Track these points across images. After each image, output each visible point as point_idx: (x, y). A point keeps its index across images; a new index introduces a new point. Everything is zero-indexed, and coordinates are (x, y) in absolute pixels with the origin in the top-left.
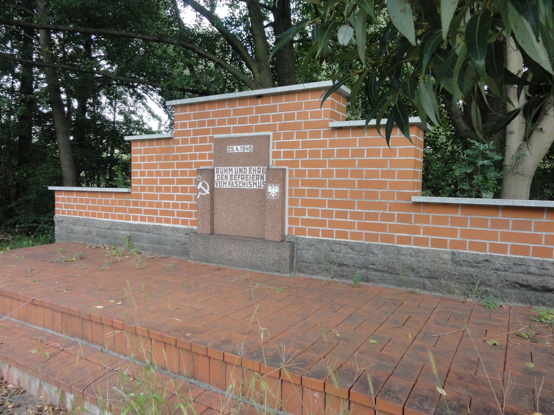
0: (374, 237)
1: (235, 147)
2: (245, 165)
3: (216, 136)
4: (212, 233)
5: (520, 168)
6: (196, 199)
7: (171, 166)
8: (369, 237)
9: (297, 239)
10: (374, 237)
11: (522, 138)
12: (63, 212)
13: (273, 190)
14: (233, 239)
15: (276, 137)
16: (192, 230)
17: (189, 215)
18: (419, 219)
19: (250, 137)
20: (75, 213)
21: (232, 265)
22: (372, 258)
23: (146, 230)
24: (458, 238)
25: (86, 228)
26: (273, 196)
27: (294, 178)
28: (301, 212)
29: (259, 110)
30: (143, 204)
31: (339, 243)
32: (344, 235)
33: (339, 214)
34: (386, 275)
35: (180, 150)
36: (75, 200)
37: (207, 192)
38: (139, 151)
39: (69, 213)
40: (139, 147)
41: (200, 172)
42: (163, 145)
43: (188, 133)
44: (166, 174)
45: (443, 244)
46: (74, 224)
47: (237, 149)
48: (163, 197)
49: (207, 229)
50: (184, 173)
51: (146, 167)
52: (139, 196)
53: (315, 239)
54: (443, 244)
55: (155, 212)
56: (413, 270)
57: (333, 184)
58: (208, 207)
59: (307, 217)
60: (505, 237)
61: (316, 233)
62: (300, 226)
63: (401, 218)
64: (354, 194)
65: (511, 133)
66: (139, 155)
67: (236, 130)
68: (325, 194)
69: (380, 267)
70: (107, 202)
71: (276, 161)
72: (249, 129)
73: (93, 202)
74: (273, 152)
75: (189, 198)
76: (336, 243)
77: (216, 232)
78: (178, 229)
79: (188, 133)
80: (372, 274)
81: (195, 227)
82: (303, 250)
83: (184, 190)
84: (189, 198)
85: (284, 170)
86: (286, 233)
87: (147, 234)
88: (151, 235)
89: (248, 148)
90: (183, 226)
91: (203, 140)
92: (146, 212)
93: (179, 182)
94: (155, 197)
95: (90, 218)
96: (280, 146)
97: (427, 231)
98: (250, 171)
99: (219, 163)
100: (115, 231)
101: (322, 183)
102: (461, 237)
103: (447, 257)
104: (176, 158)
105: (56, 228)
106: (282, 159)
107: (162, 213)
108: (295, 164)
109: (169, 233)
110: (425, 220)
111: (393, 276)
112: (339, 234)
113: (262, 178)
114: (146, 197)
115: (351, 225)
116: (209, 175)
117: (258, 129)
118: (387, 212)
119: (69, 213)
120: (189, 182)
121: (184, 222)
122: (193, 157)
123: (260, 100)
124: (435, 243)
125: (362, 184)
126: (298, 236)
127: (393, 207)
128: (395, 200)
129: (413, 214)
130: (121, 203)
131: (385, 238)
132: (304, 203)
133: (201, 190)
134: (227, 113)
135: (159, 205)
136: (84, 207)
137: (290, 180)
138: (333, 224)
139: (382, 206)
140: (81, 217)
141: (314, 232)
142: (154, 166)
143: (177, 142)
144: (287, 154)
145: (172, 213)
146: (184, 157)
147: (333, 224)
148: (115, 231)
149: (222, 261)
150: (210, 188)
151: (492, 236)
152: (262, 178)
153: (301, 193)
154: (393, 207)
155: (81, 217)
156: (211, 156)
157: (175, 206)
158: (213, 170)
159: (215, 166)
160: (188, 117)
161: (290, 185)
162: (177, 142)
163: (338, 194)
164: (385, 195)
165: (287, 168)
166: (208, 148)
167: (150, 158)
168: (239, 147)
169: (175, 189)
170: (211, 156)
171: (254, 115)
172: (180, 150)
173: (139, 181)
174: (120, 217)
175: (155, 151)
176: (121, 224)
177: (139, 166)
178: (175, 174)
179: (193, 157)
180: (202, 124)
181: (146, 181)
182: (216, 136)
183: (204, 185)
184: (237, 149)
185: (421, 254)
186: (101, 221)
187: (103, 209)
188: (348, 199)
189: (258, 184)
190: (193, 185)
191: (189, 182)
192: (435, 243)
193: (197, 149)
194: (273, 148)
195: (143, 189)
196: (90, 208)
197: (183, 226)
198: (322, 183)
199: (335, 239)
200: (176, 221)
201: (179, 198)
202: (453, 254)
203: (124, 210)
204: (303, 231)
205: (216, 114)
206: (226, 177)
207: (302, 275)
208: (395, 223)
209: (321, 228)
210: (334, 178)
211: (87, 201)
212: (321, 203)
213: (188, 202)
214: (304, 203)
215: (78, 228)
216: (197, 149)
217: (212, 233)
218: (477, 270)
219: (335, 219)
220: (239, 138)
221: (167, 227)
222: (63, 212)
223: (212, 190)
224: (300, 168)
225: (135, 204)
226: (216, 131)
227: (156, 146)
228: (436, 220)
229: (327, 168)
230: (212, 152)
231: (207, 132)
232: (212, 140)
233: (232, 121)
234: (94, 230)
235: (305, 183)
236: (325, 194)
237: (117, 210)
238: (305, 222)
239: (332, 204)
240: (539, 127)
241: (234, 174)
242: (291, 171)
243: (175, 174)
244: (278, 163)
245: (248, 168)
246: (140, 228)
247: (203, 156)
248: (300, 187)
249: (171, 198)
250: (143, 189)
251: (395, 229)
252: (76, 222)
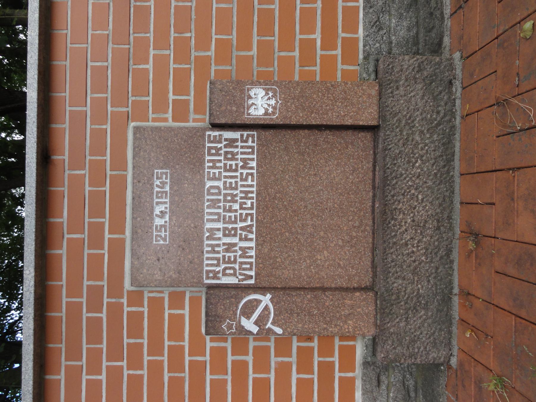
1: (158, 222)
16: (366, 364)
21: (449, 218)
26: (273, 102)
37: (266, 300)
53: (366, 14)
59: (317, 36)
62: (339, 52)
71: (196, 112)
74: (174, 120)
77: (367, 281)
82: (391, 43)
98: (214, 179)
113: (231, 143)
126: (361, 56)
149: (442, 252)
150: (255, 292)
158: (210, 287)
168: (157, 210)
171: (85, 172)
194: (166, 120)
206: (230, 247)
213: (294, 376)
223: (262, 289)
224: (212, 53)
241: (220, 225)
245: (209, 184)
248: (254, 52)
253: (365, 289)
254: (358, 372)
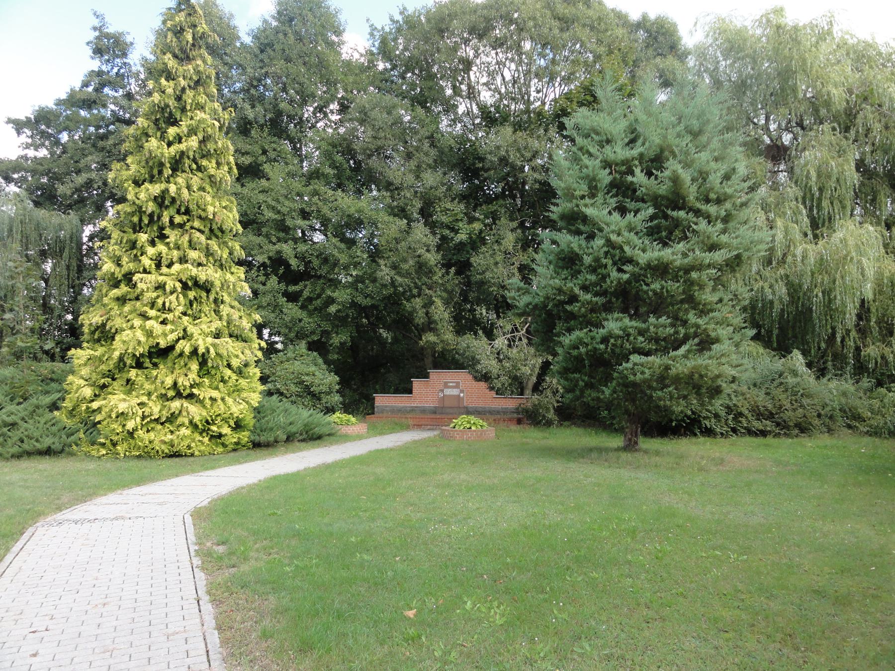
13: (462, 395)
47: (451, 384)
89: (454, 384)
116: (442, 391)
184: (451, 384)
189: (457, 393)
246: (416, 407)
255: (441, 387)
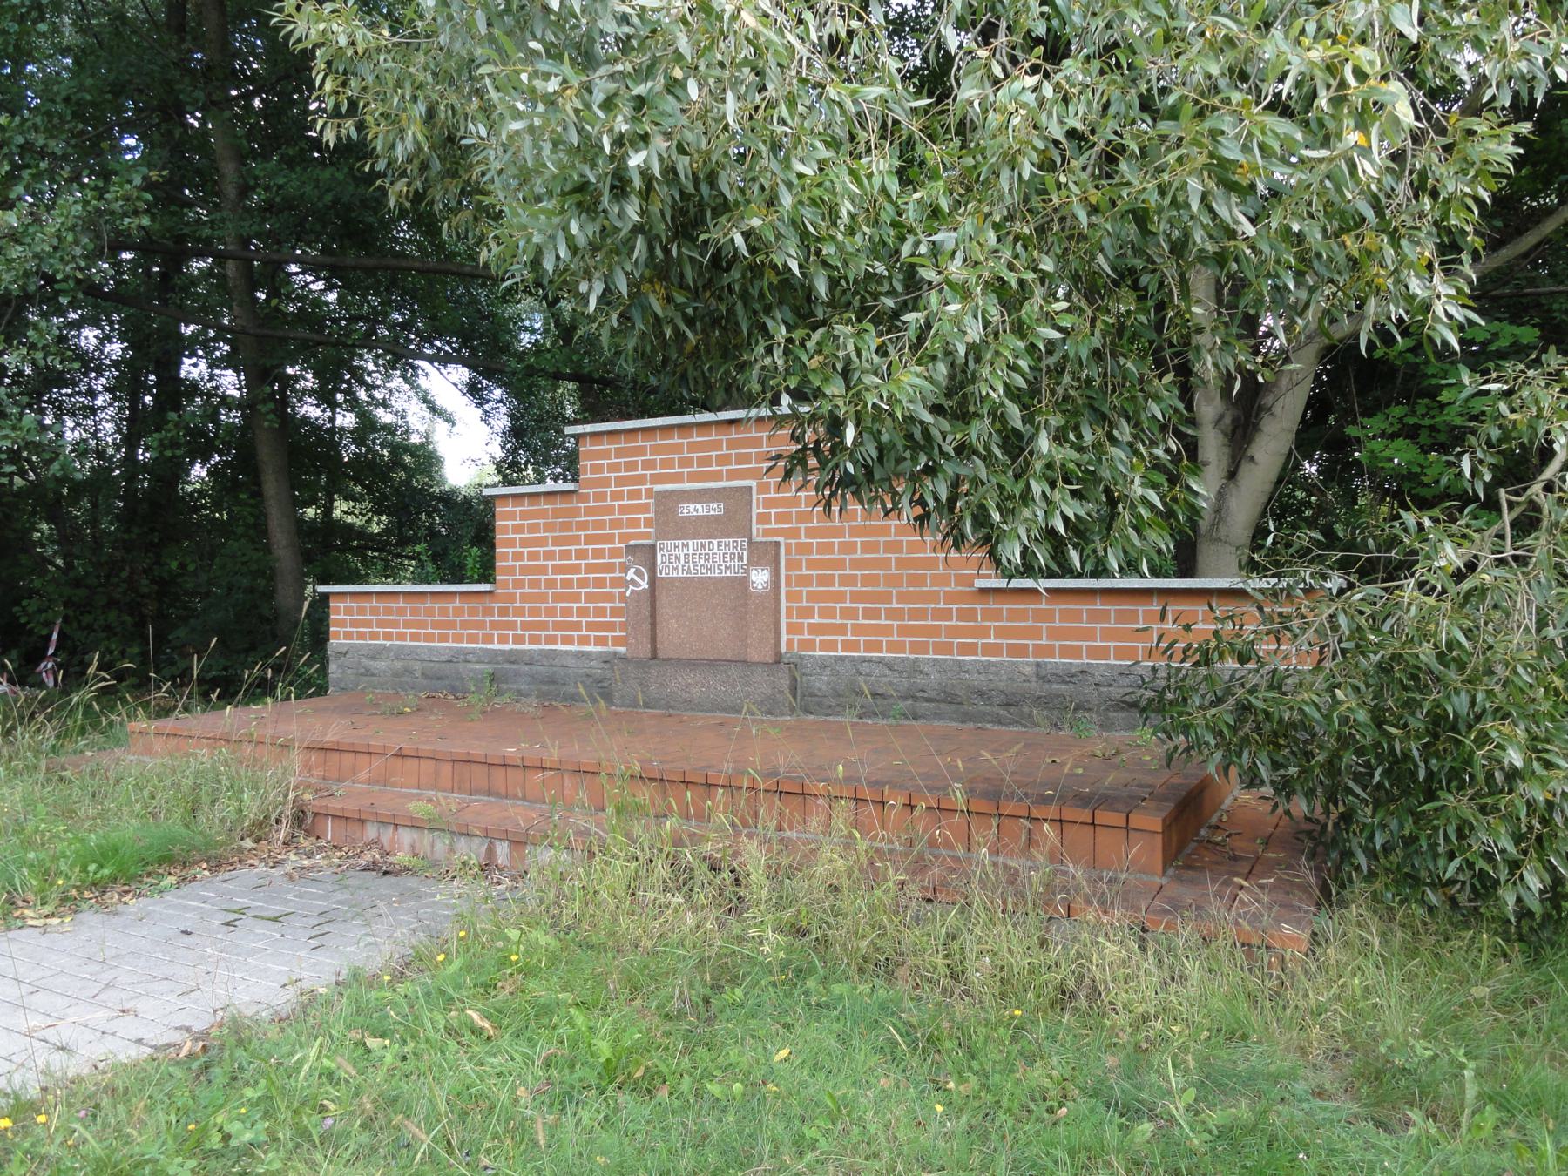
0: (923, 648)
1: (692, 507)
2: (711, 536)
3: (658, 488)
4: (654, 657)
5: (1223, 531)
6: (622, 596)
7: (575, 540)
8: (915, 647)
9: (801, 657)
10: (923, 648)
11: (1224, 474)
12: (348, 636)
13: (760, 578)
14: (692, 664)
15: (763, 488)
16: (615, 653)
17: (610, 627)
18: (987, 615)
19: (718, 490)
20: (374, 636)
22: (920, 681)
23: (526, 659)
24: (1044, 642)
25: (398, 665)
27: (794, 556)
28: (808, 613)
29: (732, 444)
30: (519, 612)
31: (870, 661)
32: (876, 646)
33: (868, 614)
34: (942, 706)
35: (590, 511)
36: (375, 611)
37: (645, 585)
38: (512, 516)
39: (361, 636)
40: (510, 509)
41: (631, 550)
42: (559, 504)
43: (605, 482)
44: (565, 555)
45: (1021, 651)
46: (374, 658)
48: (558, 598)
49: (644, 650)
50: (598, 554)
51: (525, 543)
52: (511, 598)
54: (1021, 651)
55: (543, 626)
56: (981, 694)
57: (856, 564)
58: (646, 611)
59: (816, 620)
60: (1108, 635)
61: (831, 646)
62: (806, 636)
63: (962, 614)
64: (892, 580)
65: (1206, 464)
66: (510, 523)
67: (693, 477)
68: (846, 580)
69: (933, 694)
70: (444, 612)
72: (716, 476)
73: (415, 612)
75: (609, 597)
76: (863, 660)
77: (661, 654)
78: (589, 653)
79: (605, 482)
80: (923, 706)
81: (622, 650)
83: (599, 583)
84: (609, 597)
85: (777, 544)
86: (783, 649)
87: (527, 668)
88: (534, 668)
89: (716, 508)
90: (599, 649)
91: (635, 494)
92: (525, 626)
93: (590, 568)
94: (542, 598)
95: (408, 643)
96: (769, 503)
97: (1001, 632)
99: (662, 535)
100: (461, 666)
101: (839, 564)
102: (1048, 638)
103: (1029, 670)
104: (583, 526)
105: (333, 667)
106: (773, 526)
107: (557, 626)
108: (794, 533)
109: (571, 662)
110: (997, 615)
111: (953, 707)
112: (870, 646)
113: (741, 557)
114: (525, 598)
115: (886, 630)
116: (647, 555)
117: (733, 475)
118: (941, 606)
119: (361, 636)
120: (610, 568)
121: (601, 641)
122: (616, 524)
123: (733, 428)
124: (1015, 650)
125: (901, 563)
127: (950, 597)
128: (952, 587)
129: (979, 606)
130: (473, 612)
131: (939, 648)
132: (812, 597)
133: (633, 582)
134: (677, 448)
135: (551, 612)
136: (395, 624)
137: (787, 561)
138: (859, 630)
139: (934, 598)
140: (388, 643)
141: (831, 646)
142: (542, 542)
143: (585, 498)
144: (781, 518)
145: (576, 626)
146: (599, 525)
147: (859, 630)
148: (461, 666)
151: (1088, 634)
152: (741, 557)
153: (806, 580)
154: (950, 597)
155: (388, 643)
156: (648, 523)
157: (583, 612)
158: (653, 547)
159: (657, 539)
160: (605, 454)
161: (787, 569)
162: (585, 498)
163: (867, 580)
164: (937, 580)
165: (781, 540)
166: (645, 508)
167: (534, 528)
168: (699, 506)
169: (583, 583)
170: (648, 523)
171: (725, 451)
172: (590, 511)
173: (511, 571)
174: (472, 639)
175: (542, 514)
176: (473, 652)
177: (511, 543)
178: (581, 554)
179: (616, 524)
180: (631, 466)
181: (524, 570)
182: (658, 488)
183: (638, 573)
185: (993, 669)
186: (431, 649)
187: (436, 625)
188: (882, 588)
189: (735, 569)
190: (617, 574)
191: (610, 568)
192: (1015, 650)
193: (623, 509)
195: (519, 584)
196: (407, 624)
197: (599, 649)
198: (839, 564)
199: (862, 654)
200: (584, 640)
201: (590, 598)
202: (1038, 665)
203: (480, 625)
204: (808, 644)
205: (656, 450)
206: (678, 558)
207: (812, 717)
208: (954, 623)
209: (840, 638)
210: (858, 555)
211: (401, 611)
212: (840, 597)
214: (812, 597)
215: (381, 665)
216: (623, 509)
217: (654, 657)
218: (1072, 687)
219: (861, 621)
220: (699, 491)
221: (566, 652)
222: (348, 636)
223: (653, 581)
224: (804, 540)
225: (504, 612)
226: (658, 479)
227: (544, 506)
228: (1013, 615)
229: (847, 539)
230: (652, 515)
231: (641, 480)
232: (649, 493)
233: (685, 463)
234: (417, 666)
235: (812, 564)
236: (846, 580)
237: (465, 625)
238: (814, 629)
239: (856, 597)
240: (1249, 453)
242: (788, 546)
243: (581, 554)
244: (766, 533)
246: (512, 658)
247: (634, 523)
248: (805, 572)
249: (575, 598)
250: (519, 584)
251: (953, 632)
252: (376, 654)
253: (654, 650)
254: (611, 649)
255: (643, 532)
